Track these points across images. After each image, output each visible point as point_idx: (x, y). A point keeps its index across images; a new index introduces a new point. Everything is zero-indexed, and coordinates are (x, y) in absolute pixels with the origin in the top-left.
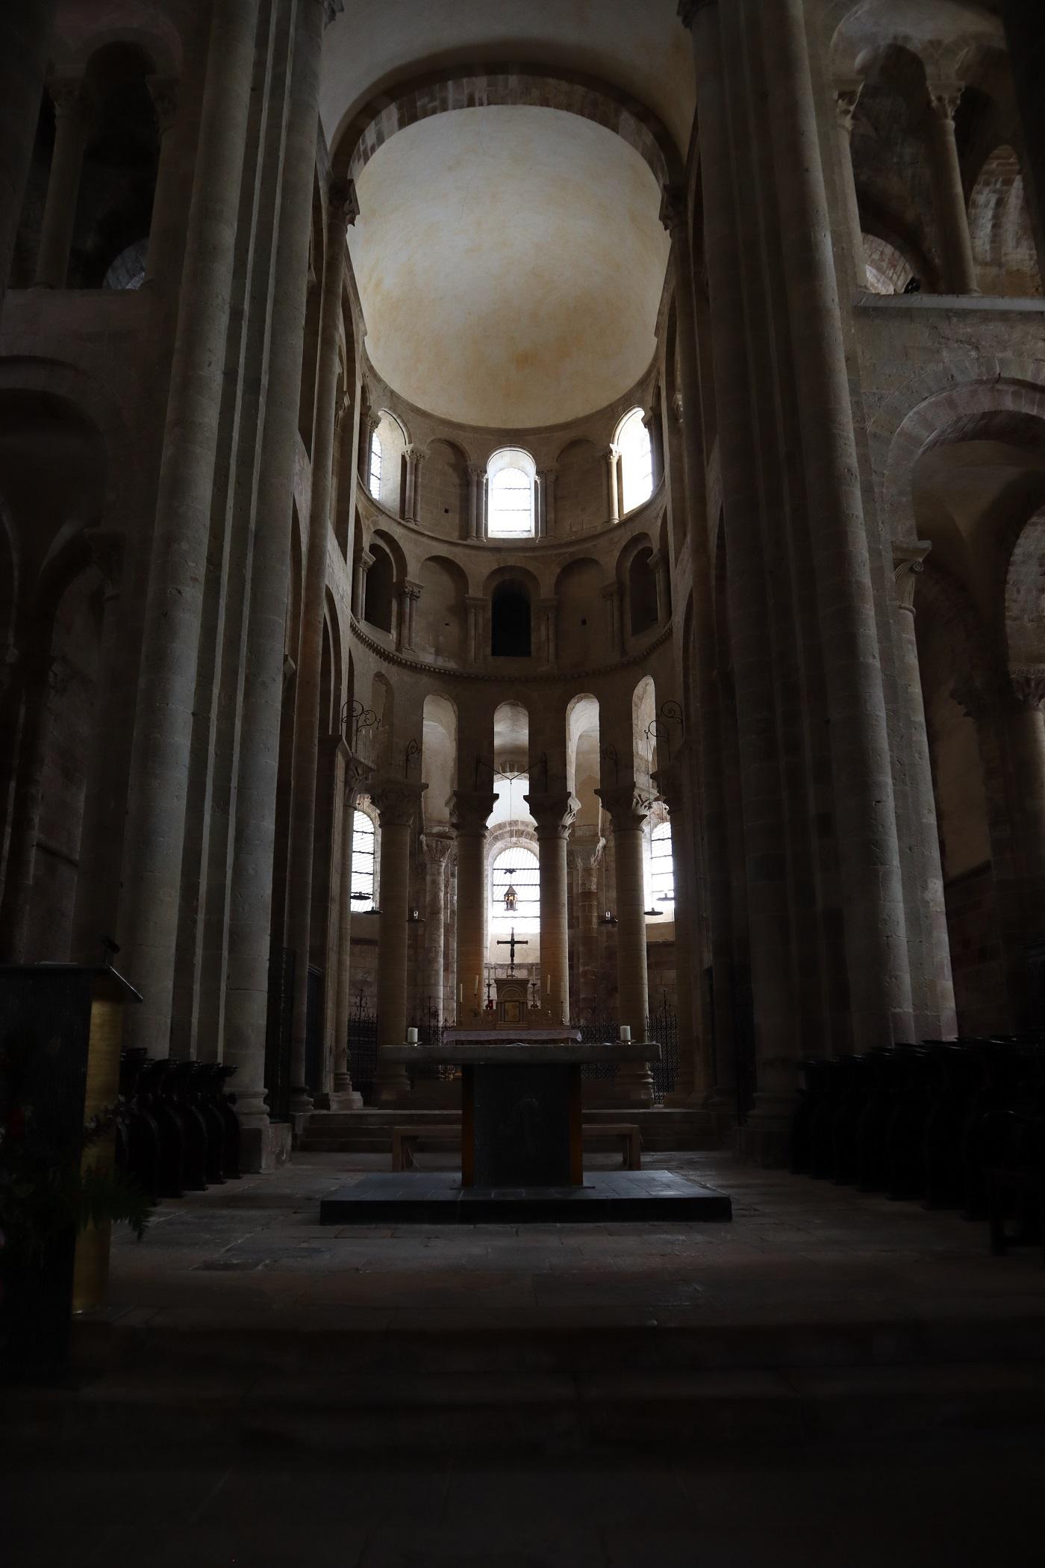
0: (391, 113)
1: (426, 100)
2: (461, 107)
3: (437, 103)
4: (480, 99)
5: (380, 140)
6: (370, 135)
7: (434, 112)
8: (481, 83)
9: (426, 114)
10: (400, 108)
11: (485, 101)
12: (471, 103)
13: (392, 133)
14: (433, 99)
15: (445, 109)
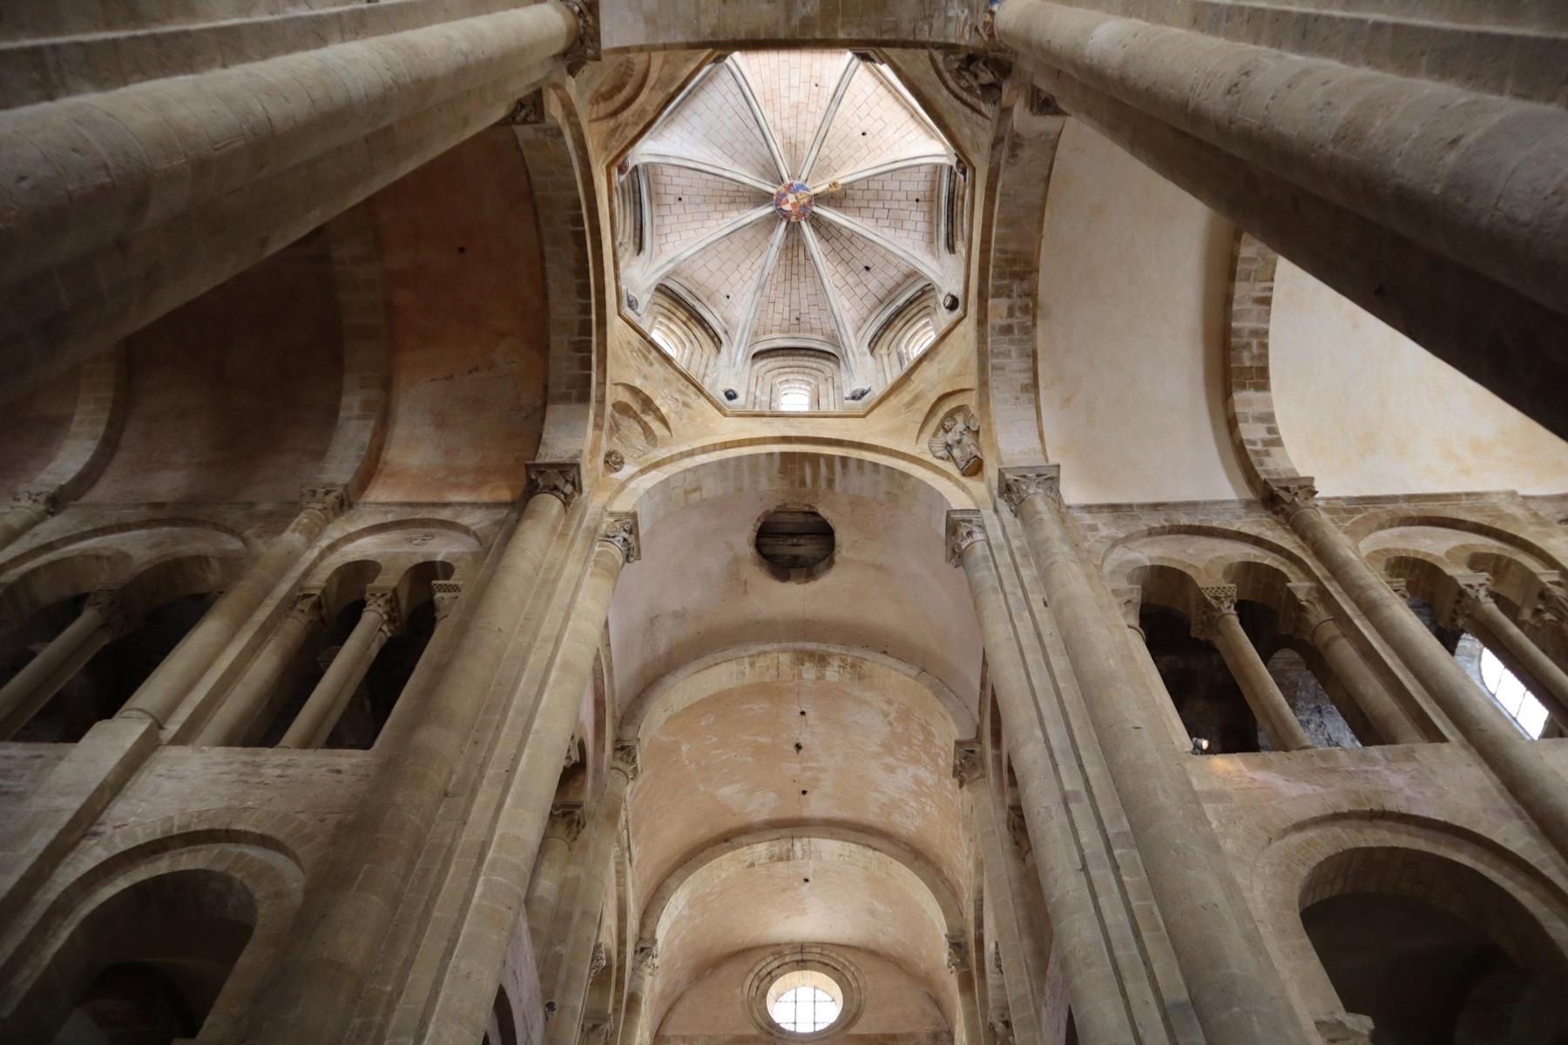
0: (1245, 400)
1: (1246, 355)
2: (1268, 313)
3: (1255, 342)
4: (1264, 290)
5: (1268, 418)
6: (1251, 432)
7: (1264, 346)
8: (1241, 289)
9: (1264, 355)
10: (1243, 387)
11: (1268, 284)
12: (1266, 301)
13: (1269, 402)
14: (1248, 346)
15: (1266, 333)
